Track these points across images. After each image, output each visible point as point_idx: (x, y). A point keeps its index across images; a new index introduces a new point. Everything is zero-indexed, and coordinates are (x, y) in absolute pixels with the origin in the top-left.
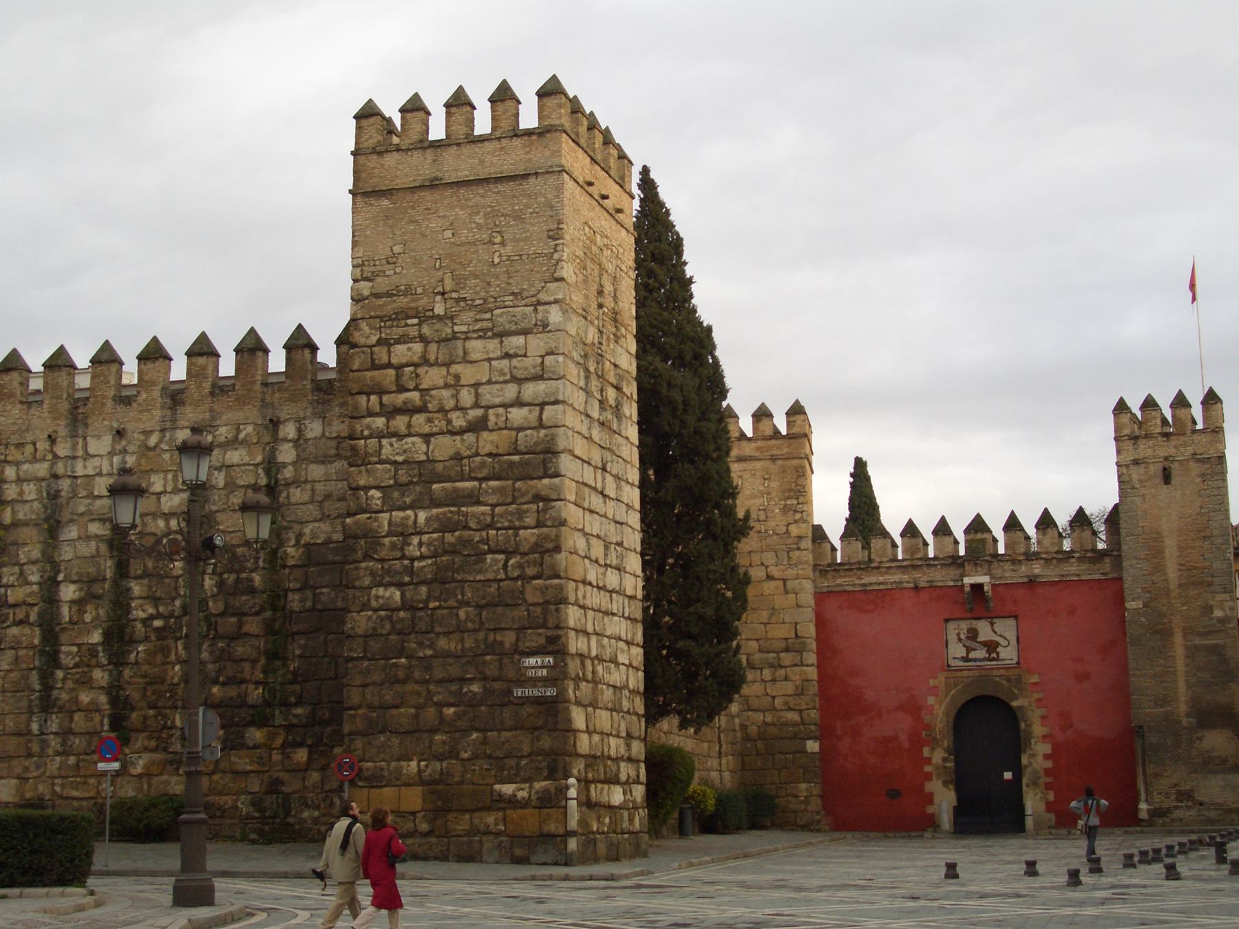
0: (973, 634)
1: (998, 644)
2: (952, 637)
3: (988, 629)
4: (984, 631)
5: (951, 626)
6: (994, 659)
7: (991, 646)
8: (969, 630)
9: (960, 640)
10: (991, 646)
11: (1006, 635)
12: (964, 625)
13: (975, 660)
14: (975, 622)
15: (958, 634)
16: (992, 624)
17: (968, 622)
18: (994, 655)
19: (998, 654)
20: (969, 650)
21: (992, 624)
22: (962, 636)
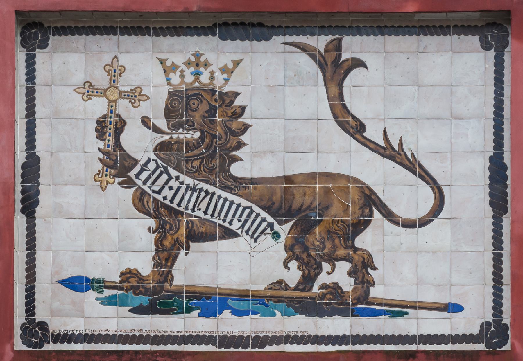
0: (208, 129)
1: (370, 200)
2: (67, 145)
3: (315, 97)
4: (283, 105)
5: (67, 67)
6: (334, 303)
7: (322, 220)
8: (180, 104)
9: (118, 165)
10: (322, 220)
11: (419, 144)
12: (150, 68)
13: (209, 301)
14: (218, 52)
15: (109, 127)
16: (335, 70)
17: (179, 49)
18: (339, 275)
19: (363, 267)
20: (175, 232)
21: (335, 70)
22: (138, 142)
